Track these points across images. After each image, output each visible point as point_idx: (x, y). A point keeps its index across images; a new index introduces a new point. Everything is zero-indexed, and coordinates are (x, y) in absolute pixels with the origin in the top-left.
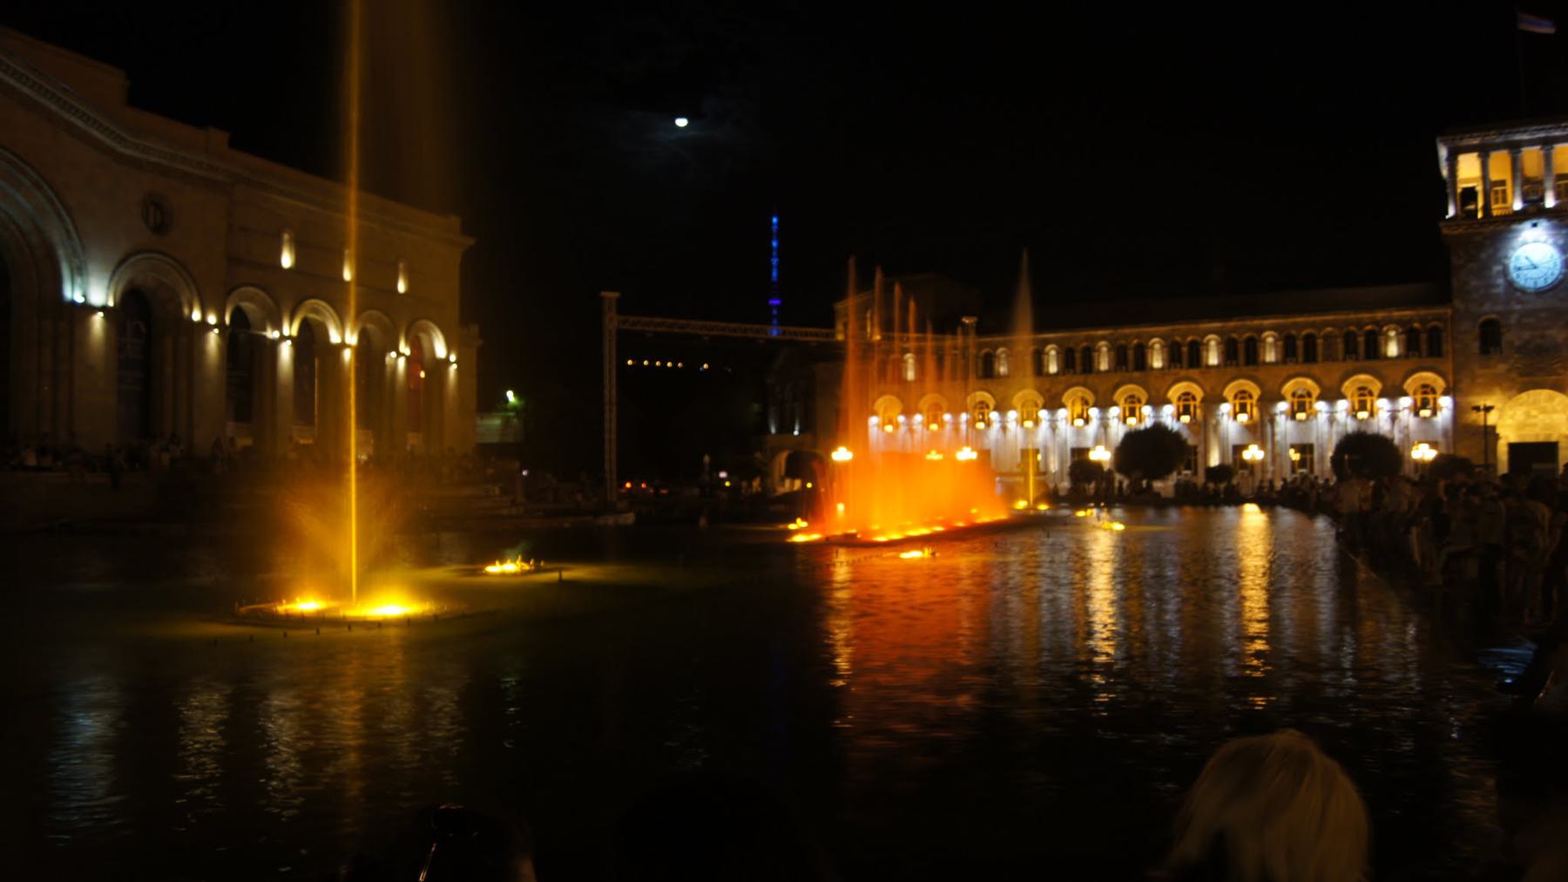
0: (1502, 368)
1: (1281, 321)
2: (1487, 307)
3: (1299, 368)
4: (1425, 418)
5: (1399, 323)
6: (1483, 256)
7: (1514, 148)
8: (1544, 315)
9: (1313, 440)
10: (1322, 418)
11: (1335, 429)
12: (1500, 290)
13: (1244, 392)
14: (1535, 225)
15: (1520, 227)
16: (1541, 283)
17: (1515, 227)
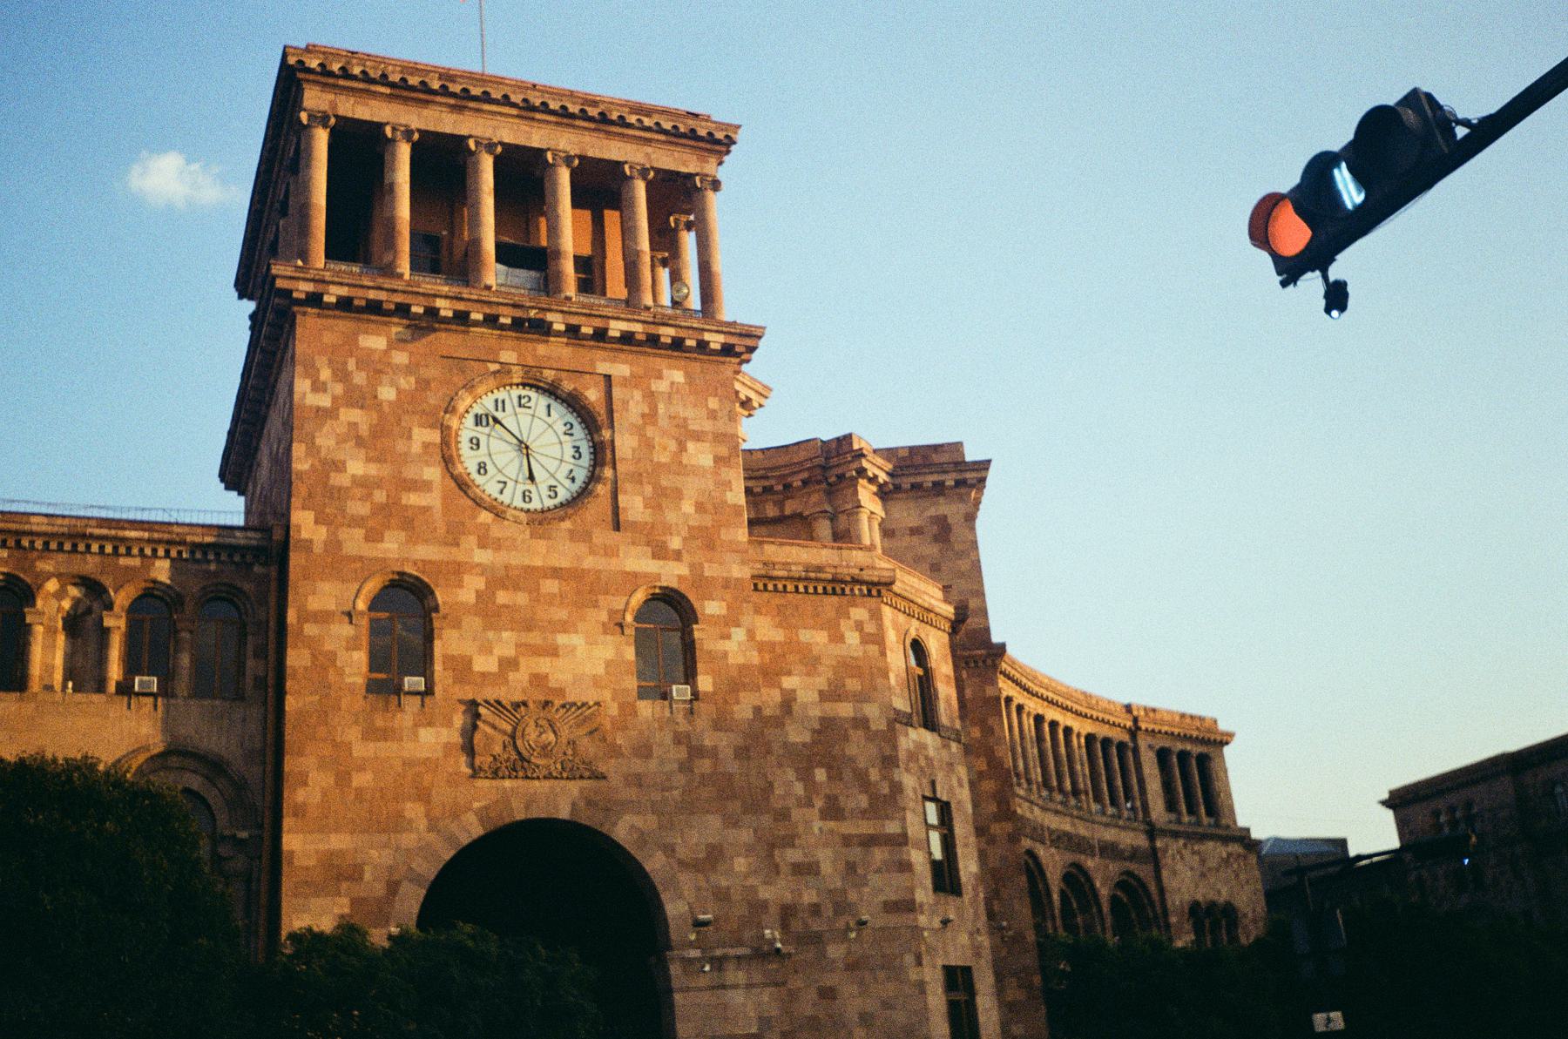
6: (387, 393)
8: (551, 586)
12: (432, 500)
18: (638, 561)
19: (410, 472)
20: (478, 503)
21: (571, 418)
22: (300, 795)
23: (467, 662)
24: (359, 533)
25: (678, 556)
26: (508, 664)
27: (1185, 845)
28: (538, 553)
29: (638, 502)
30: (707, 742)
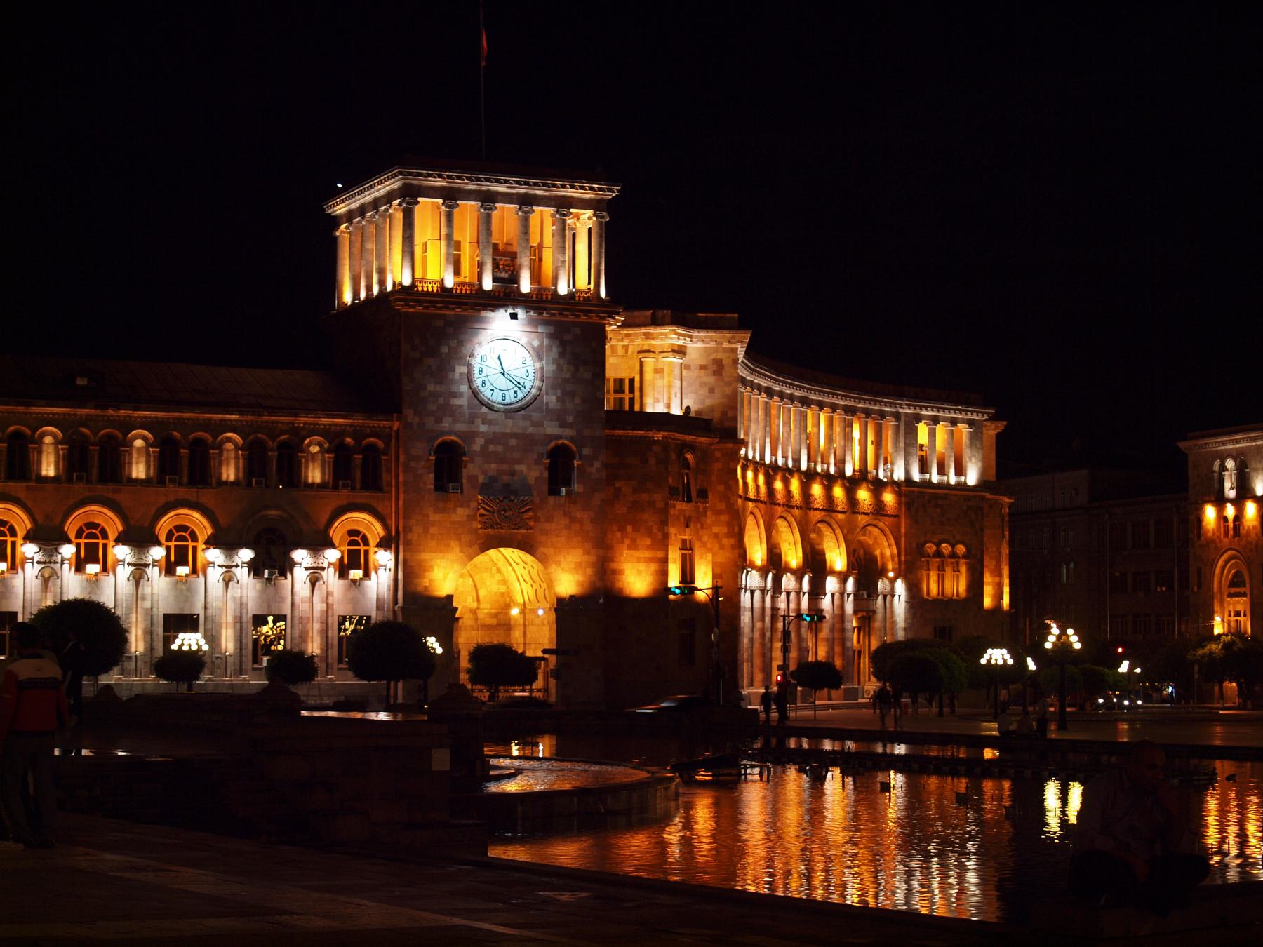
0: (461, 513)
1: (160, 414)
2: (446, 424)
3: (183, 492)
4: (354, 581)
5: (326, 433)
6: (445, 350)
7: (488, 200)
8: (513, 442)
9: (198, 609)
10: (215, 574)
11: (234, 590)
12: (462, 402)
13: (95, 526)
14: (514, 316)
15: (490, 315)
16: (510, 398)
17: (484, 314)
18: (551, 428)
19: (454, 388)
20: (482, 403)
21: (527, 355)
22: (410, 536)
23: (476, 477)
24: (432, 419)
25: (570, 426)
26: (493, 479)
27: (929, 502)
28: (508, 426)
29: (553, 399)
30: (578, 515)
